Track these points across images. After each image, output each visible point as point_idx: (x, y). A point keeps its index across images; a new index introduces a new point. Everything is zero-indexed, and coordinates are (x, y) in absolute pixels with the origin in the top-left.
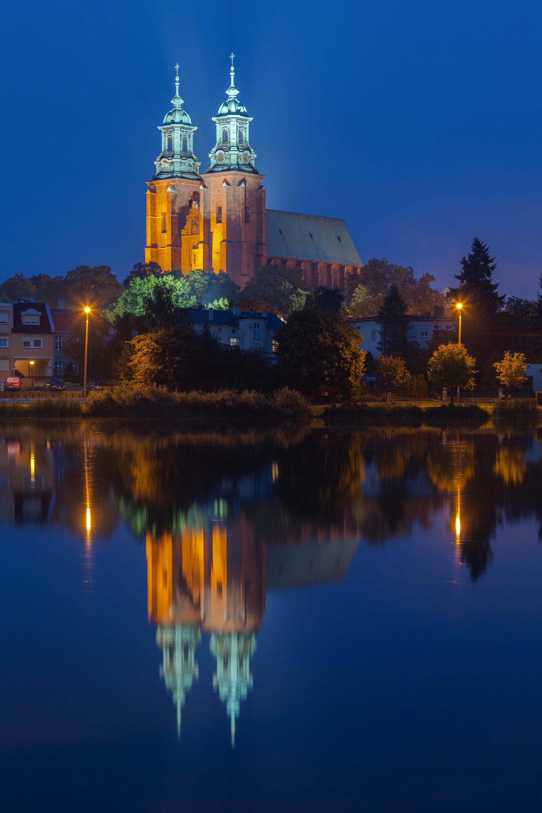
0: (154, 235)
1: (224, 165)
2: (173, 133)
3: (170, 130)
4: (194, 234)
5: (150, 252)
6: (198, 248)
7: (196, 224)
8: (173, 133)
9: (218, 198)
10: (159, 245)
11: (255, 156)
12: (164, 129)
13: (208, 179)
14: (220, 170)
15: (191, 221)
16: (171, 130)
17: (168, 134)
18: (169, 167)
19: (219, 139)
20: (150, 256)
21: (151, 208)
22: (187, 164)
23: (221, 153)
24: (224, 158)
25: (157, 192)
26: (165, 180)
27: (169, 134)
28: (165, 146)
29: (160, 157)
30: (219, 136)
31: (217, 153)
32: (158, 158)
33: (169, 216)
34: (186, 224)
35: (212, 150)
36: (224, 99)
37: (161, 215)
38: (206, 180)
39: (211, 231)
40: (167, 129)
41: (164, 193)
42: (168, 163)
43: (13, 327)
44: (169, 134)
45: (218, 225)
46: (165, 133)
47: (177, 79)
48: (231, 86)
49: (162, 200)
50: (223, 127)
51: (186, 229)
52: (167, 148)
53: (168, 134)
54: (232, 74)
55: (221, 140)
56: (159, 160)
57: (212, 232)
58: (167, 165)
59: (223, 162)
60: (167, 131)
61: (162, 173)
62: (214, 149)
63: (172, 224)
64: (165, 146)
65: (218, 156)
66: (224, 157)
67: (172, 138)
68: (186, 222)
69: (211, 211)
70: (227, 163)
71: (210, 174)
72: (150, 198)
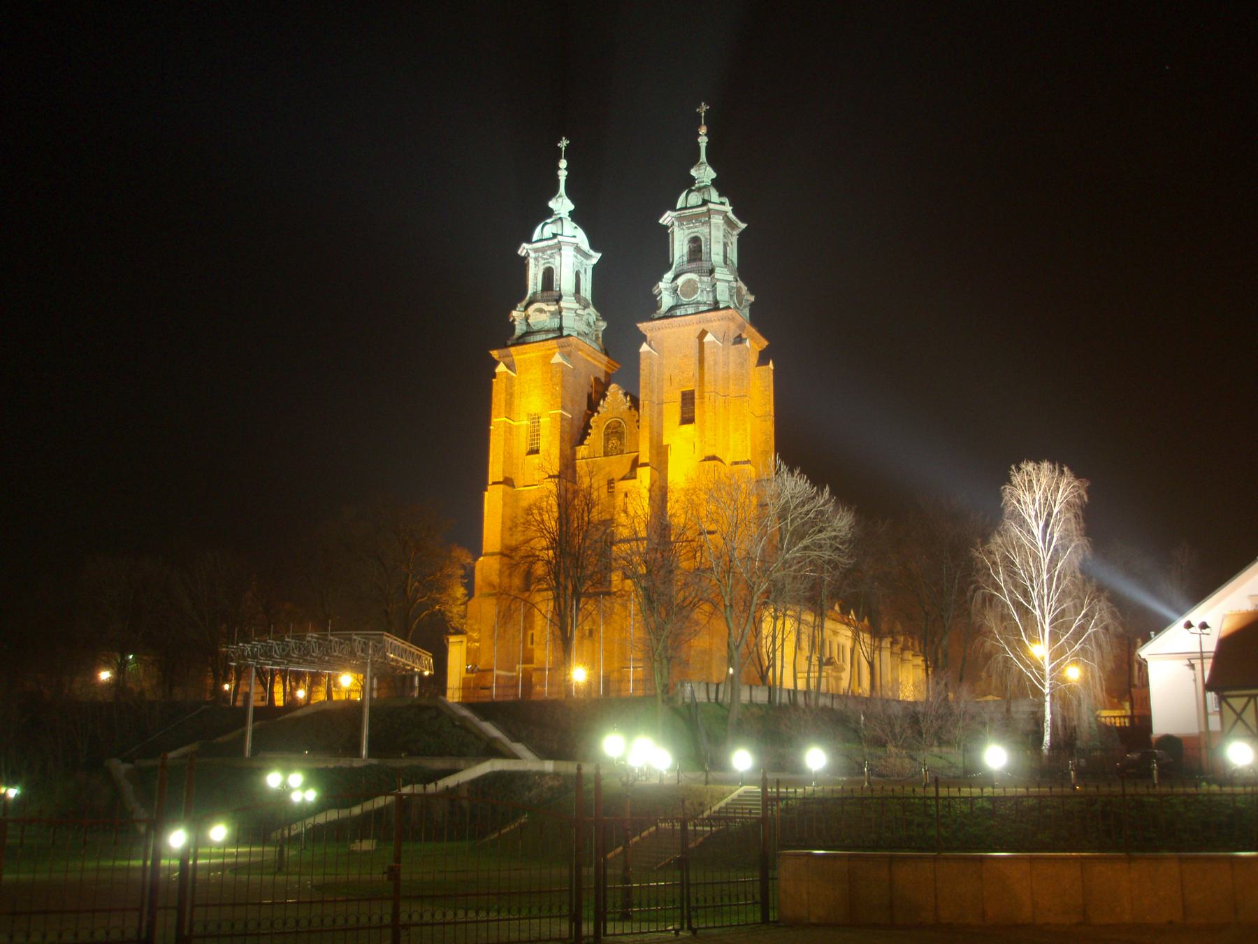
0: (509, 458)
1: (698, 303)
2: (557, 257)
3: (549, 252)
4: (612, 455)
5: (501, 493)
6: (635, 478)
7: (617, 432)
8: (557, 257)
9: (683, 372)
10: (519, 481)
11: (752, 298)
12: (536, 251)
13: (658, 334)
14: (689, 312)
15: (605, 427)
16: (553, 251)
17: (543, 262)
18: (548, 321)
19: (678, 257)
20: (501, 501)
21: (506, 401)
22: (584, 318)
23: (689, 281)
24: (699, 291)
25: (517, 372)
26: (542, 343)
27: (546, 261)
28: (536, 284)
29: (524, 303)
30: (679, 248)
31: (680, 281)
32: (520, 306)
33: (556, 414)
34: (589, 434)
35: (665, 276)
36: (689, 183)
37: (525, 418)
38: (651, 336)
39: (665, 443)
40: (543, 250)
41: (534, 371)
42: (545, 312)
43: (572, 207)
44: (546, 261)
45: (685, 427)
46: (536, 259)
47: (563, 164)
48: (701, 161)
49: (530, 387)
50: (691, 233)
51: (588, 445)
52: (540, 288)
53: (543, 262)
54: (703, 141)
55: (685, 259)
56: (523, 309)
57: (668, 445)
58: (543, 317)
59: (693, 299)
60: (540, 254)
61: (529, 333)
62: (669, 276)
63: (561, 432)
64: (536, 284)
65: (682, 286)
66: (697, 288)
67: (553, 267)
68: (589, 431)
69: (665, 401)
70: (705, 299)
71: (665, 321)
72: (505, 380)
